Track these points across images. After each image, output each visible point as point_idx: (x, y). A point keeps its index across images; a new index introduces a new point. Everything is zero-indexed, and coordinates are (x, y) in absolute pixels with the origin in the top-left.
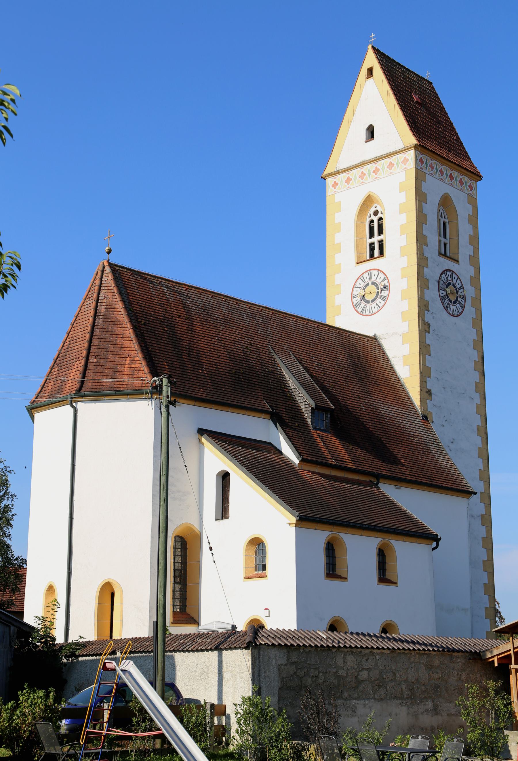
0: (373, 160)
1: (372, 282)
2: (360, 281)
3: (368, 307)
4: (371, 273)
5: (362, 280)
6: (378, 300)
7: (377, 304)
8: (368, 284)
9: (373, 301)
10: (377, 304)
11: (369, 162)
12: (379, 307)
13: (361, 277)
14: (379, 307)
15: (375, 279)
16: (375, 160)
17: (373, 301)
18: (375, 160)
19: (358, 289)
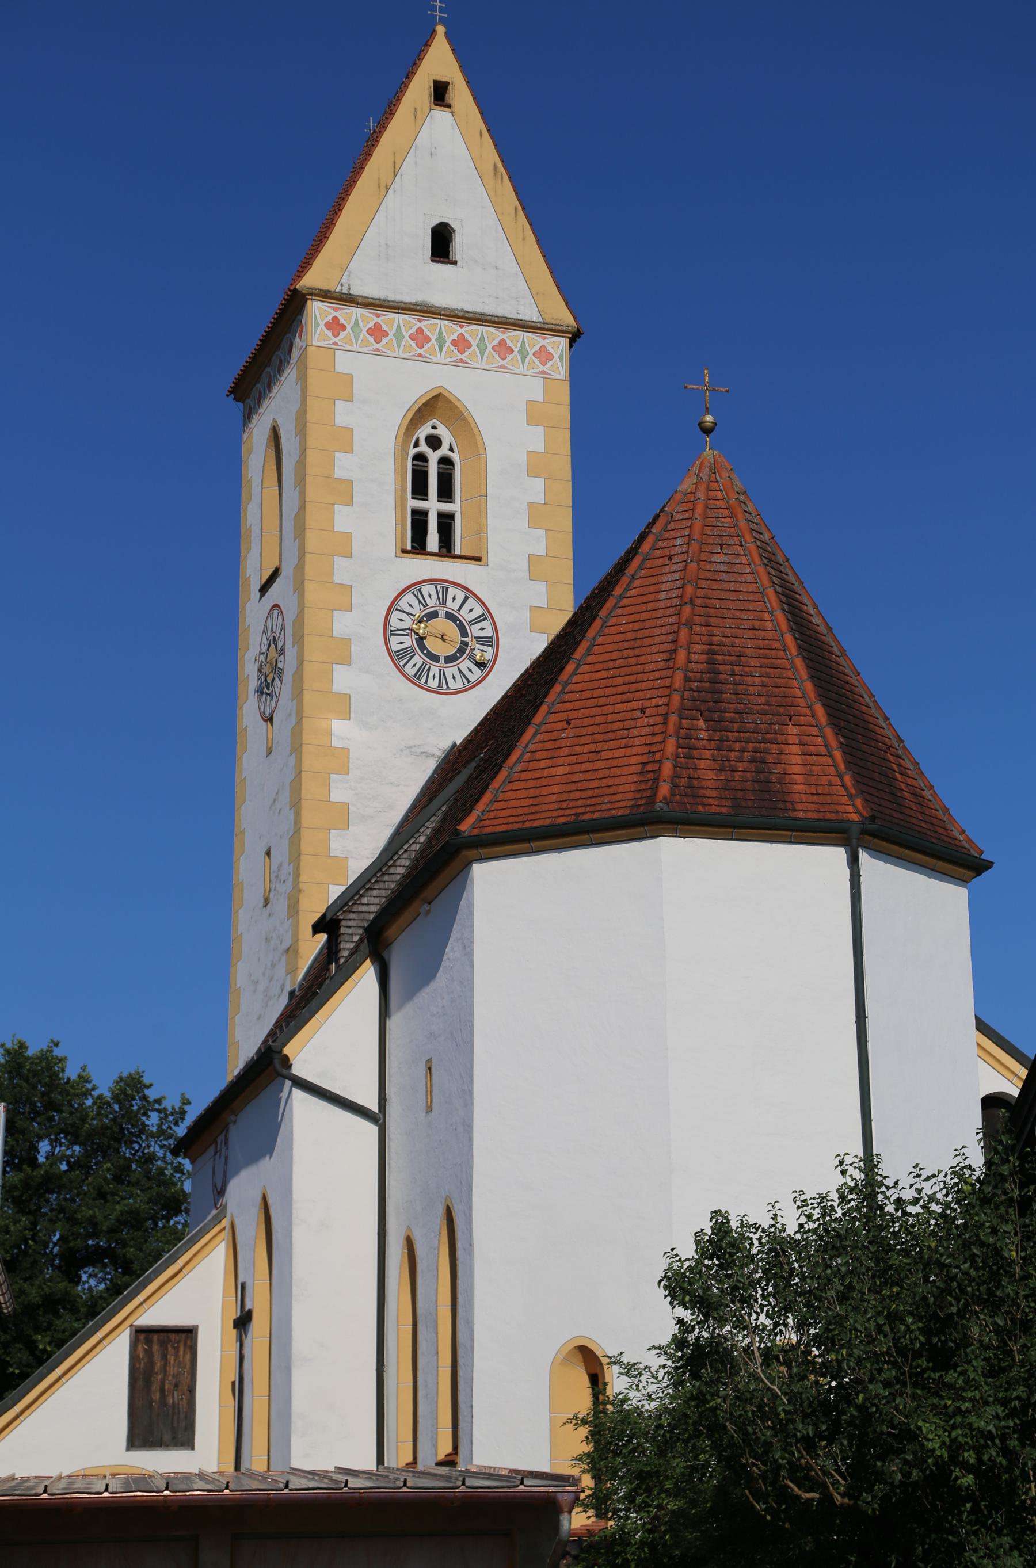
0: (460, 314)
1: (447, 613)
2: (409, 598)
3: (435, 670)
4: (445, 591)
5: (417, 598)
6: (465, 664)
7: (461, 672)
8: (434, 615)
9: (449, 659)
10: (461, 672)
11: (444, 315)
12: (469, 681)
13: (414, 587)
14: (469, 681)
15: (456, 608)
16: (463, 317)
17: (449, 659)
18: (463, 317)
19: (404, 616)
